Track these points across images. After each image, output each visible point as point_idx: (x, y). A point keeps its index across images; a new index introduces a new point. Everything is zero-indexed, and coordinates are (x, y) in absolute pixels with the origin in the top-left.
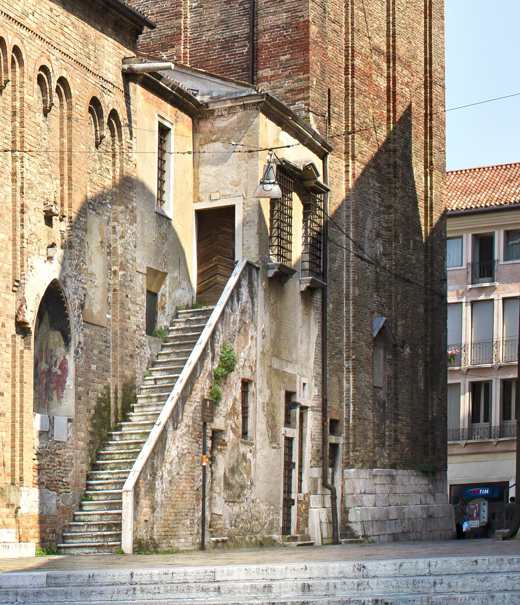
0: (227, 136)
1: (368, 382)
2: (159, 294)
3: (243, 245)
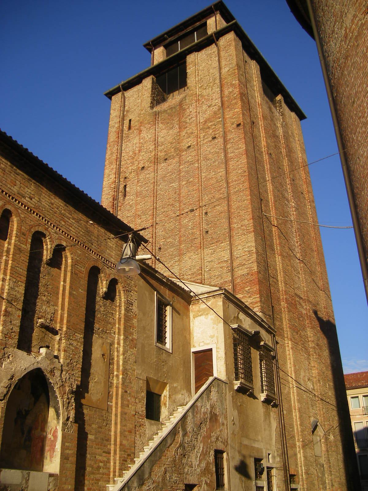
0: (206, 312)
1: (311, 454)
2: (163, 395)
3: (217, 370)
